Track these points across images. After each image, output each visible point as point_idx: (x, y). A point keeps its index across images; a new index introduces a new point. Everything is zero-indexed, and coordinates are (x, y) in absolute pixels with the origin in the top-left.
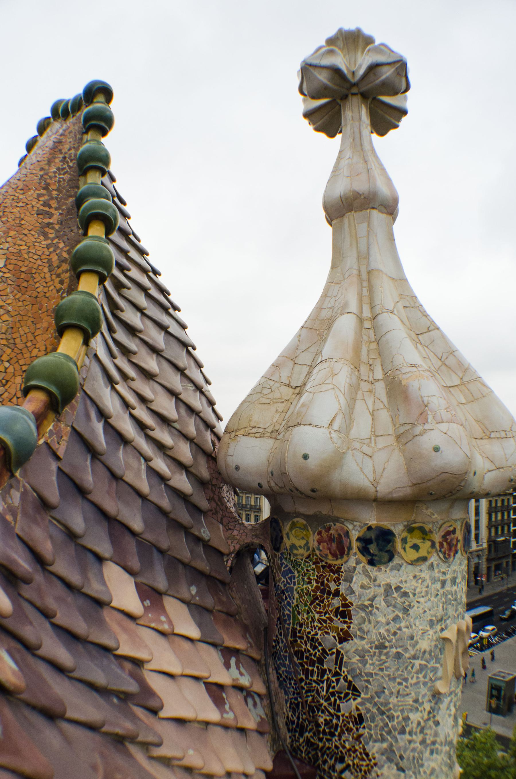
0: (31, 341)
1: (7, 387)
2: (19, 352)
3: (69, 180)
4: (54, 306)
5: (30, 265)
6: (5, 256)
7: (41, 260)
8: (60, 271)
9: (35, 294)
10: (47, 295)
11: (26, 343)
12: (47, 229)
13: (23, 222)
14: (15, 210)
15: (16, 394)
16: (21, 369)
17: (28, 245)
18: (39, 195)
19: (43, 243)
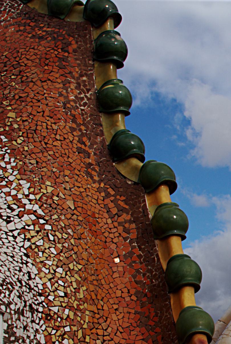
0: (112, 282)
1: (108, 322)
2: (107, 292)
3: (91, 115)
4: (124, 253)
5: (93, 209)
6: (71, 198)
7: (99, 204)
8: (121, 219)
9: (104, 239)
10: (115, 241)
11: (109, 284)
12: (90, 170)
13: (70, 160)
14: (55, 143)
15: (118, 329)
16: (113, 307)
17: (84, 188)
18: (73, 129)
19: (94, 185)
